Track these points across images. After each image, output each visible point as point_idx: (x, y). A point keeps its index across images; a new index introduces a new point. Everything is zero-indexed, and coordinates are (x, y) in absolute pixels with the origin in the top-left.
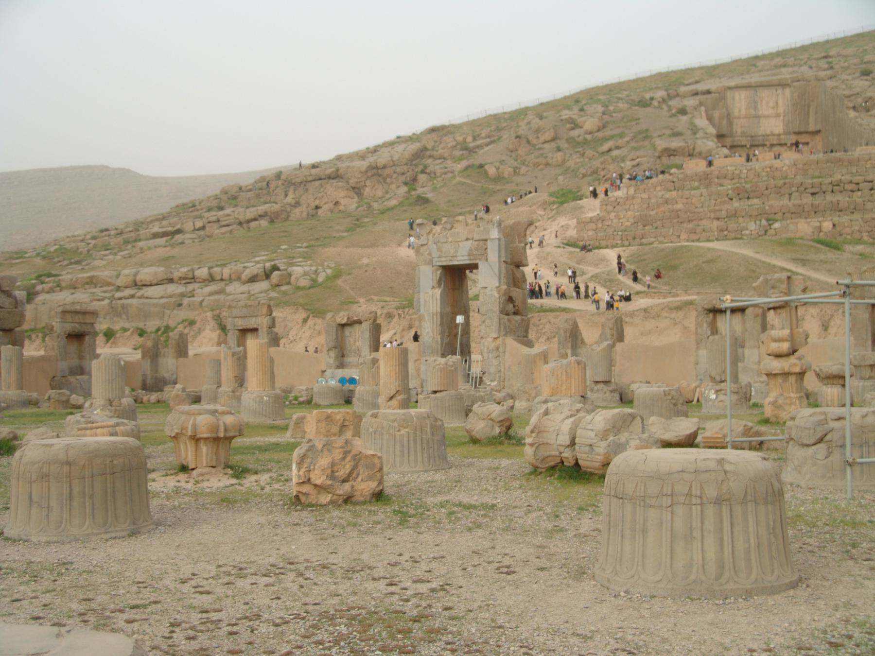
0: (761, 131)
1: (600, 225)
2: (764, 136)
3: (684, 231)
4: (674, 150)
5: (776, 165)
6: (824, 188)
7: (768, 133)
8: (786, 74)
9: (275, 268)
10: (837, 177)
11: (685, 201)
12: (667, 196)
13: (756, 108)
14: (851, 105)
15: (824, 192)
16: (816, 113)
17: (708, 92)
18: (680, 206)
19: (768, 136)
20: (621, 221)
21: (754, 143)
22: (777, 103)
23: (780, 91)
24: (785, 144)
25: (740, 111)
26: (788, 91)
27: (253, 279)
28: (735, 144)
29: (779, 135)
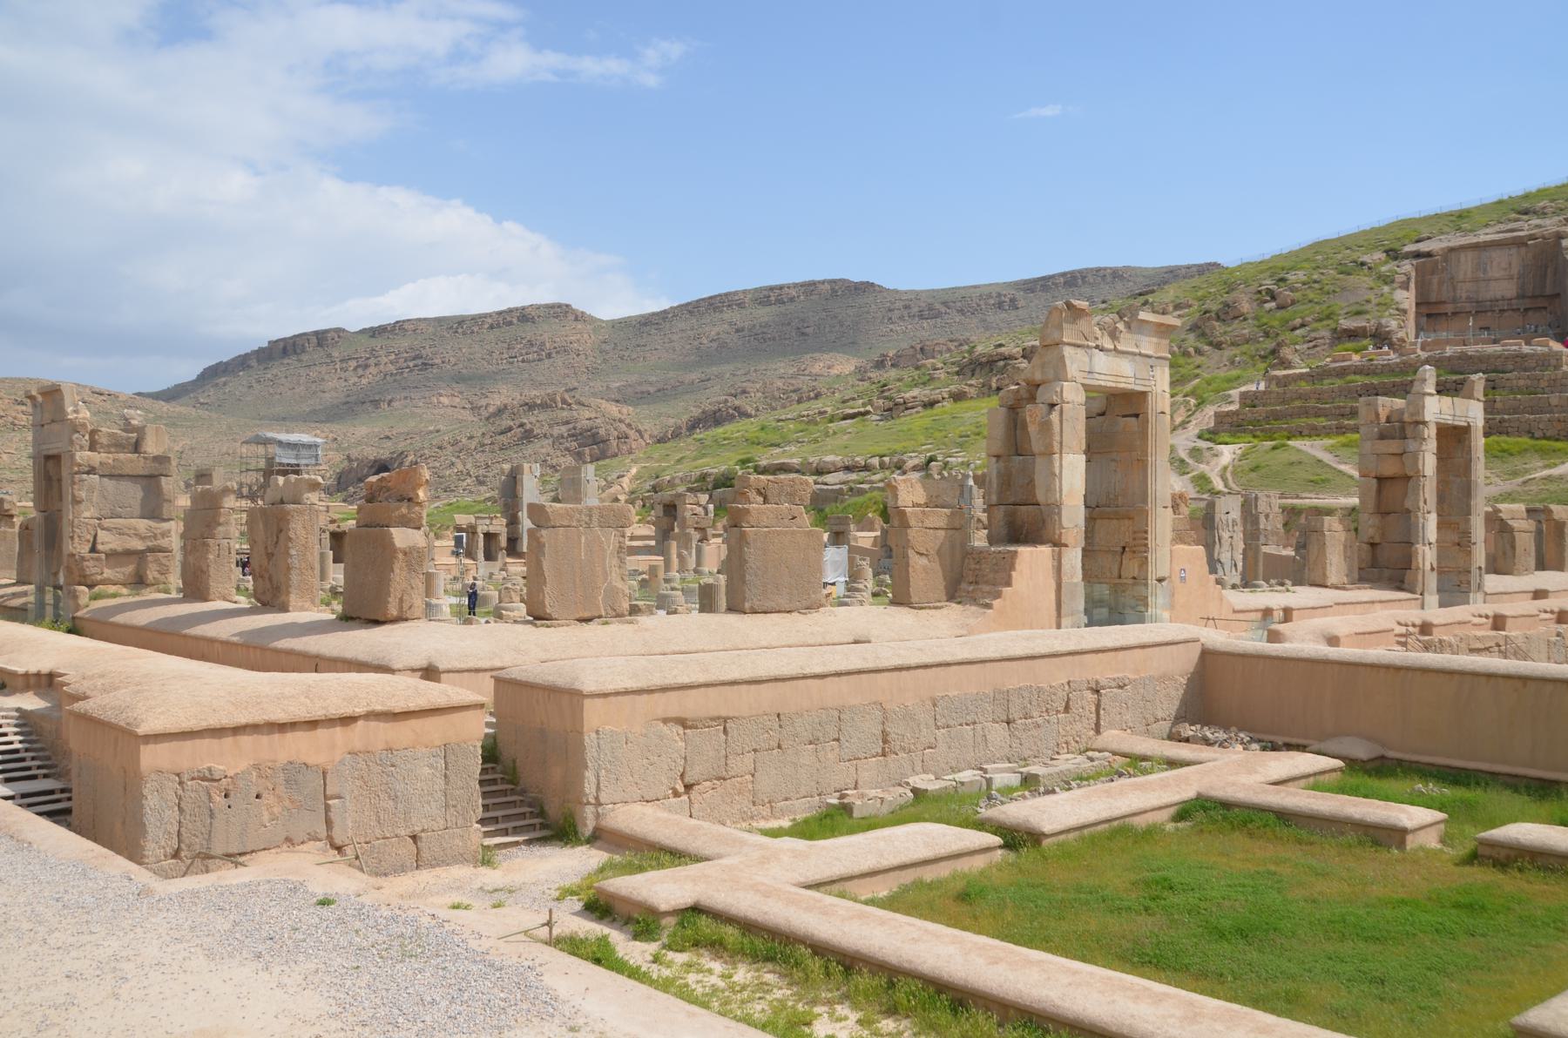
0: (1490, 295)
2: (1491, 301)
4: (1354, 331)
6: (1448, 386)
7: (1499, 297)
8: (1527, 227)
9: (931, 459)
13: (1485, 271)
17: (1429, 255)
19: (1497, 301)
21: (1480, 309)
22: (1510, 264)
24: (1519, 309)
25: (1465, 274)
26: (1523, 250)
27: (915, 468)
28: (1458, 310)
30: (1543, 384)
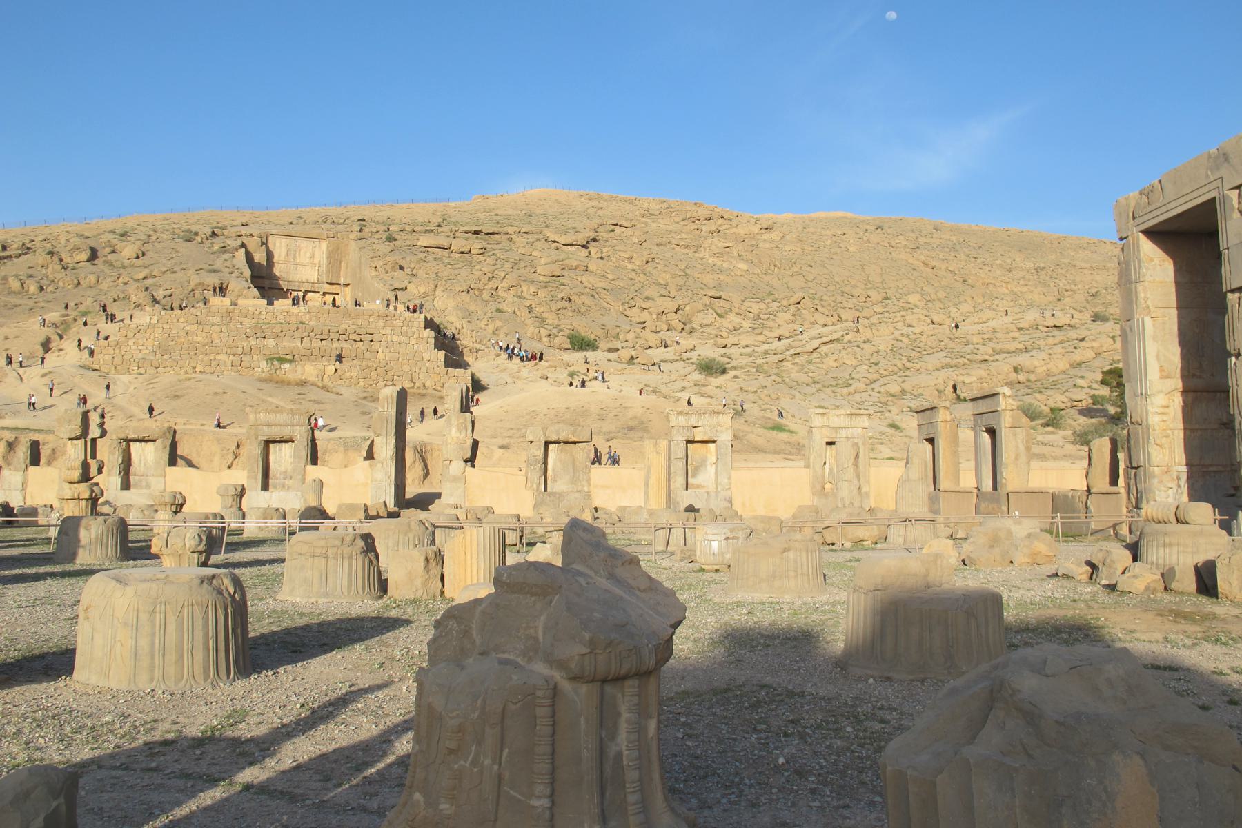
0: (297, 278)
1: (117, 351)
3: (199, 363)
5: (292, 311)
7: (304, 280)
10: (345, 326)
11: (205, 335)
12: (188, 328)
14: (374, 266)
15: (332, 340)
16: (347, 268)
18: (199, 339)
20: (140, 348)
23: (317, 242)
26: (324, 245)
28: (273, 286)
29: (313, 283)
30: (413, 342)
